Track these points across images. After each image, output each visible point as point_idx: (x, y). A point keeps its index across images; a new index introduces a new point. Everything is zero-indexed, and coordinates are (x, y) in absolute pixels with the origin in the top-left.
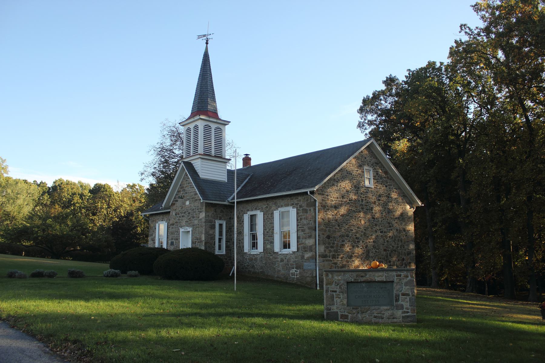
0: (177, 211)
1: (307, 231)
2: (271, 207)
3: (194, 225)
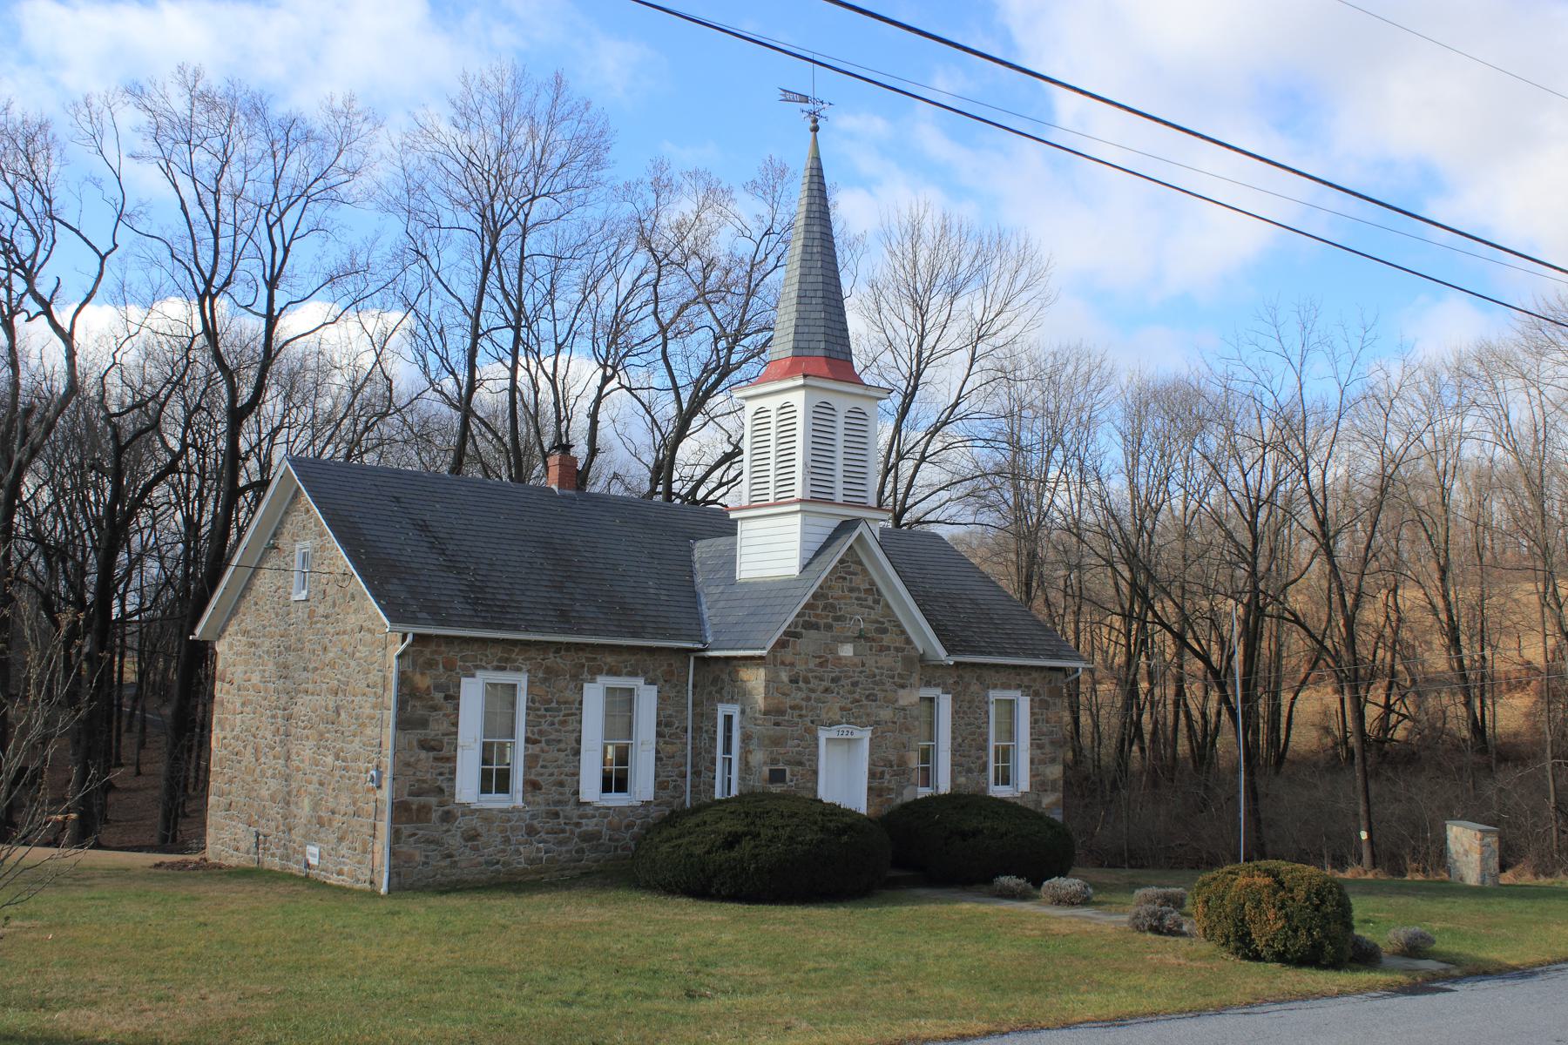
0: (800, 668)
1: (1048, 749)
2: (967, 685)
3: (877, 723)
